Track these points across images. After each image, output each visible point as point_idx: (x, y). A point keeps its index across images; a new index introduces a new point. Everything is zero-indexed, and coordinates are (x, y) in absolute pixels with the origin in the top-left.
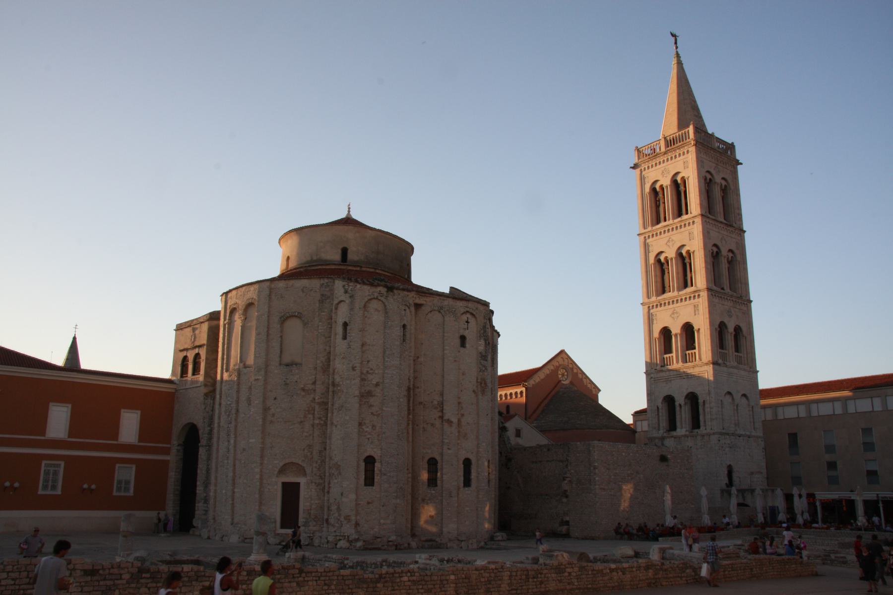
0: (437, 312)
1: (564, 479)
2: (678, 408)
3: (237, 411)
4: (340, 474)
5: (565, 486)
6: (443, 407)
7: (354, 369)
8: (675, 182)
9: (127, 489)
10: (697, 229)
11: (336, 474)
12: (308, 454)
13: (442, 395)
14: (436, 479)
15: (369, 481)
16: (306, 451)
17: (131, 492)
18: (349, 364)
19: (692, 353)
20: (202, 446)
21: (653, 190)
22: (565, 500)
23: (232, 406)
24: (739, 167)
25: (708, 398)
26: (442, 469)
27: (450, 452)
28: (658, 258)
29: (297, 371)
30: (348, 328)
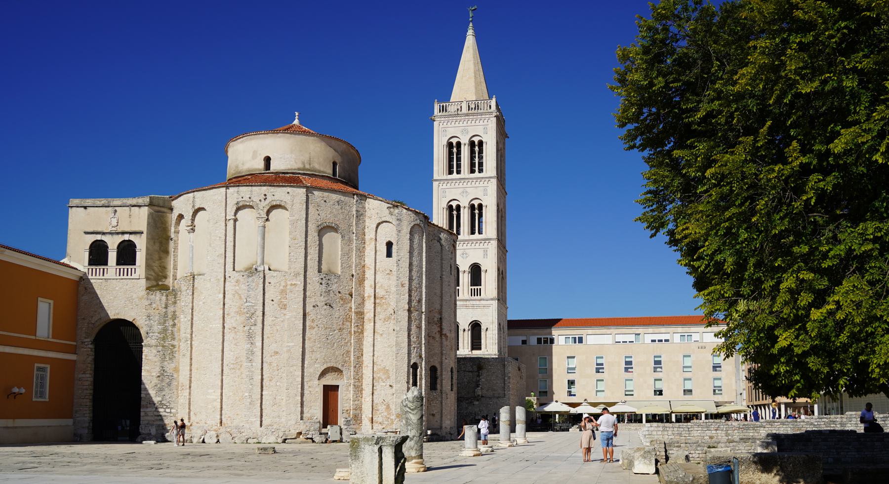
0: (436, 241)
1: (478, 386)
2: (461, 333)
3: (264, 314)
4: (389, 378)
5: (479, 392)
6: (441, 323)
7: (402, 285)
8: (472, 144)
9: (42, 395)
10: (493, 185)
11: (383, 377)
12: (347, 359)
13: (440, 313)
14: (436, 384)
15: (415, 384)
16: (344, 355)
17: (47, 400)
18: (397, 280)
19: (477, 289)
20: (150, 346)
21: (450, 145)
22: (477, 403)
23: (255, 308)
24: (506, 139)
25: (491, 326)
26: (441, 375)
27: (446, 361)
28: (450, 203)
29: (336, 280)
30: (394, 248)
